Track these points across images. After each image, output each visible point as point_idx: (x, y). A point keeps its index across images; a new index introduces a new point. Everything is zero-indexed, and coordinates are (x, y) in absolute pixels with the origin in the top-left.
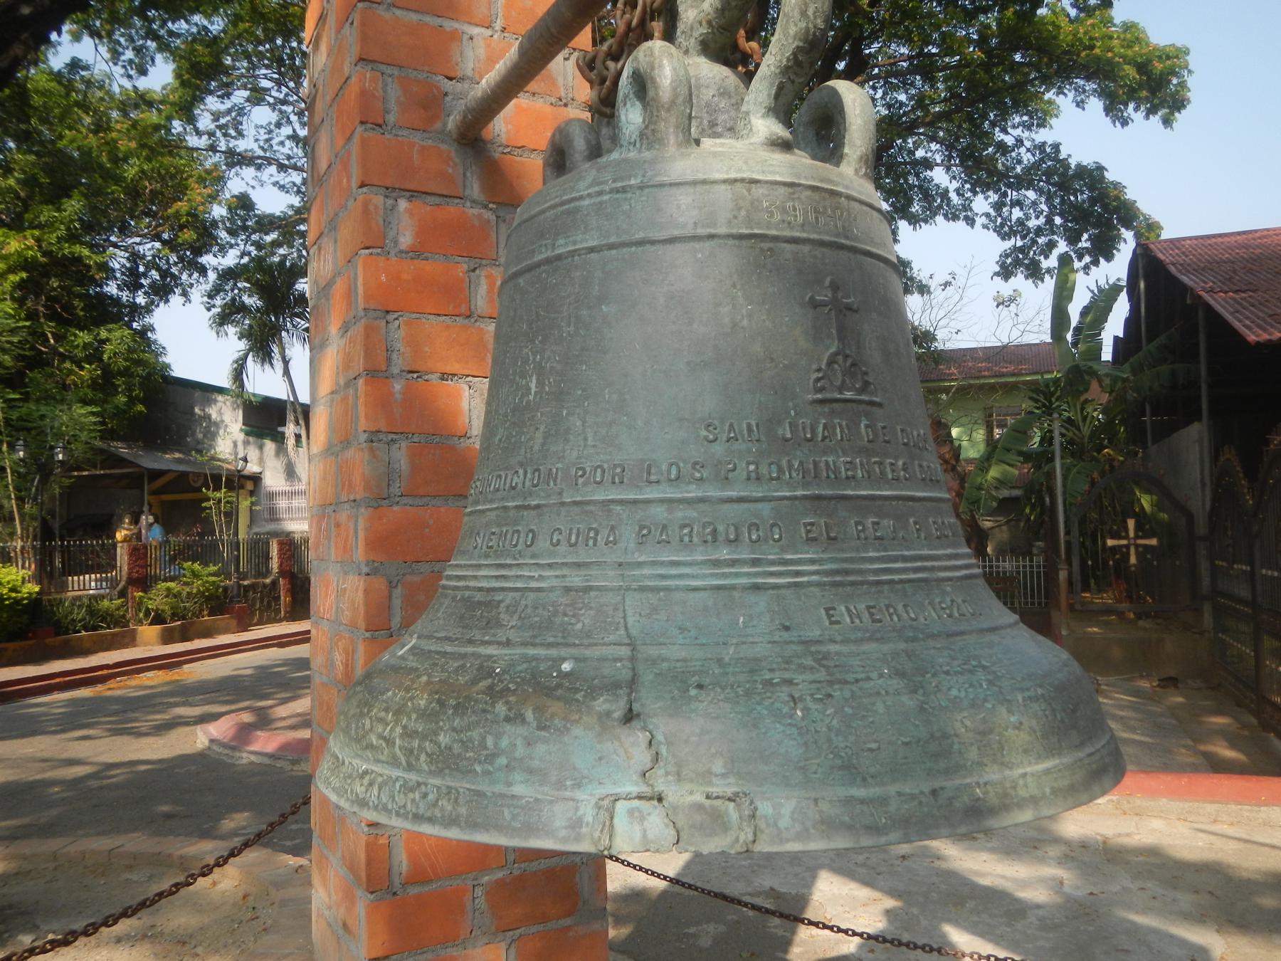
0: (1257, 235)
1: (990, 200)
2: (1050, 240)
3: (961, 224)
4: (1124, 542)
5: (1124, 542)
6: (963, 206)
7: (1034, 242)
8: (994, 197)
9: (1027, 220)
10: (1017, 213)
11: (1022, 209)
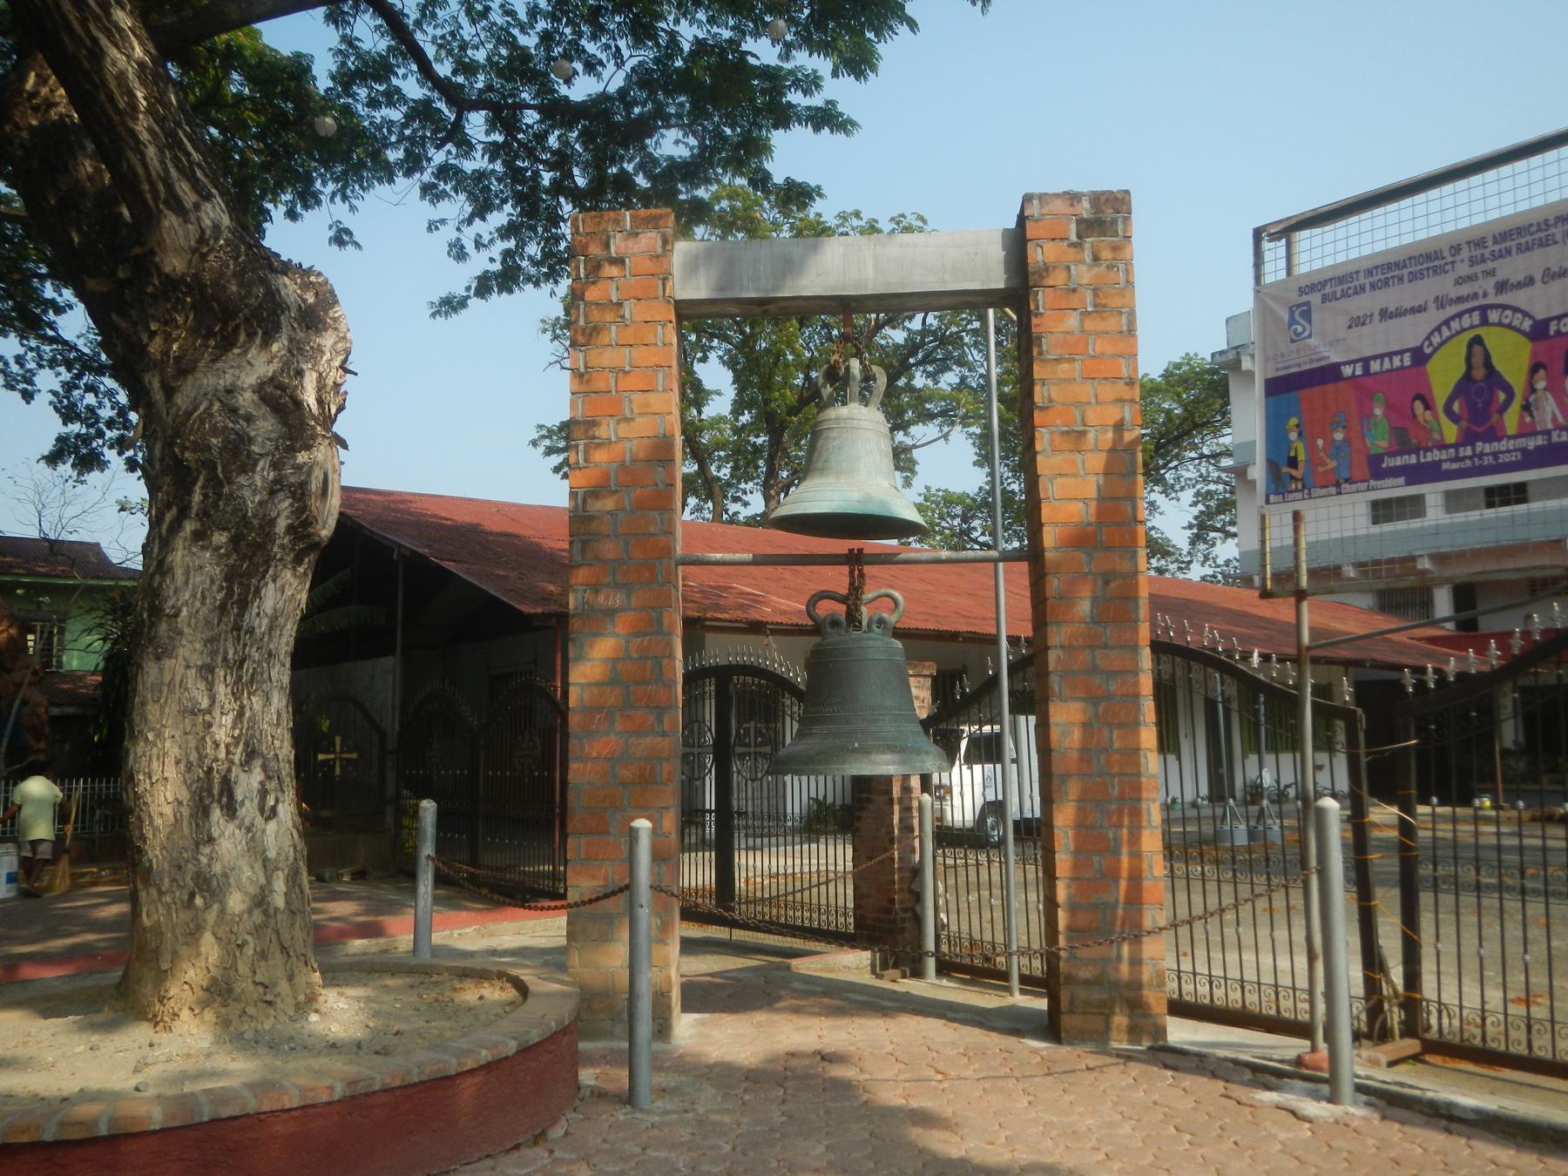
0: (392, 498)
1: (62, 378)
2: (122, 435)
3: (16, 396)
4: (331, 756)
5: (331, 756)
6: (23, 376)
7: (101, 434)
8: (66, 376)
9: (100, 407)
10: (90, 399)
11: (96, 396)
